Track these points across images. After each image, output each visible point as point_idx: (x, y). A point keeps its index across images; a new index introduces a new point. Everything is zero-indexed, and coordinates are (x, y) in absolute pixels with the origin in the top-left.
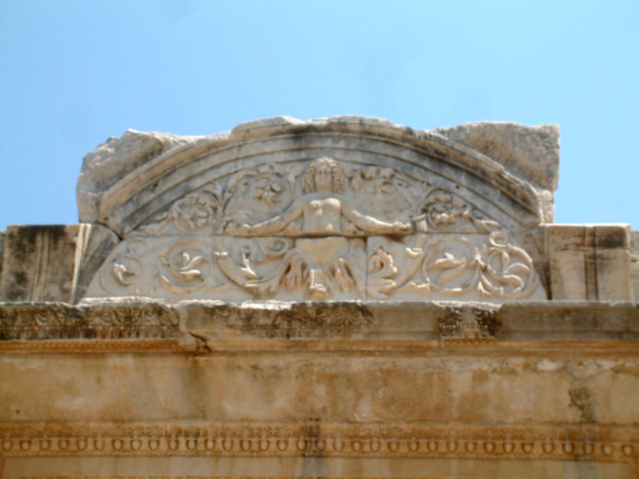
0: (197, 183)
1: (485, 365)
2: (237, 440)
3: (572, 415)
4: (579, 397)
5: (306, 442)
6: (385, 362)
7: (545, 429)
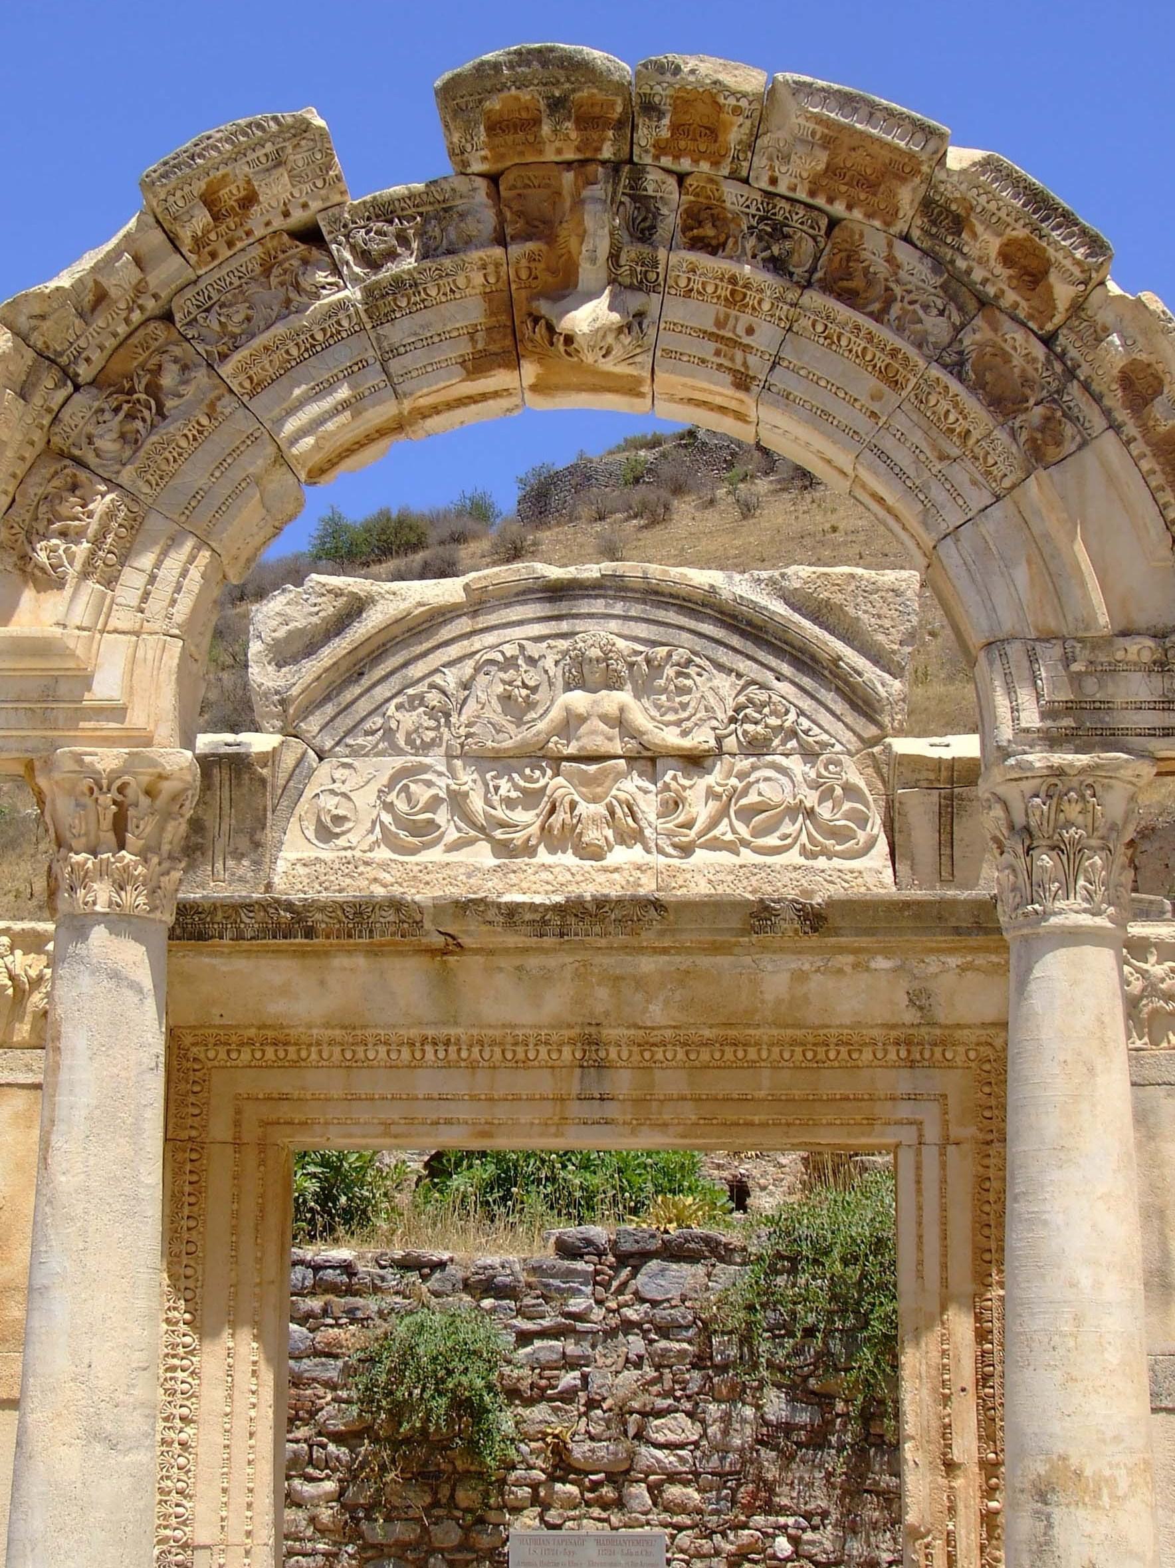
1: (806, 963)
2: (498, 1050)
3: (910, 1016)
4: (917, 999)
5: (585, 1051)
7: (875, 1032)
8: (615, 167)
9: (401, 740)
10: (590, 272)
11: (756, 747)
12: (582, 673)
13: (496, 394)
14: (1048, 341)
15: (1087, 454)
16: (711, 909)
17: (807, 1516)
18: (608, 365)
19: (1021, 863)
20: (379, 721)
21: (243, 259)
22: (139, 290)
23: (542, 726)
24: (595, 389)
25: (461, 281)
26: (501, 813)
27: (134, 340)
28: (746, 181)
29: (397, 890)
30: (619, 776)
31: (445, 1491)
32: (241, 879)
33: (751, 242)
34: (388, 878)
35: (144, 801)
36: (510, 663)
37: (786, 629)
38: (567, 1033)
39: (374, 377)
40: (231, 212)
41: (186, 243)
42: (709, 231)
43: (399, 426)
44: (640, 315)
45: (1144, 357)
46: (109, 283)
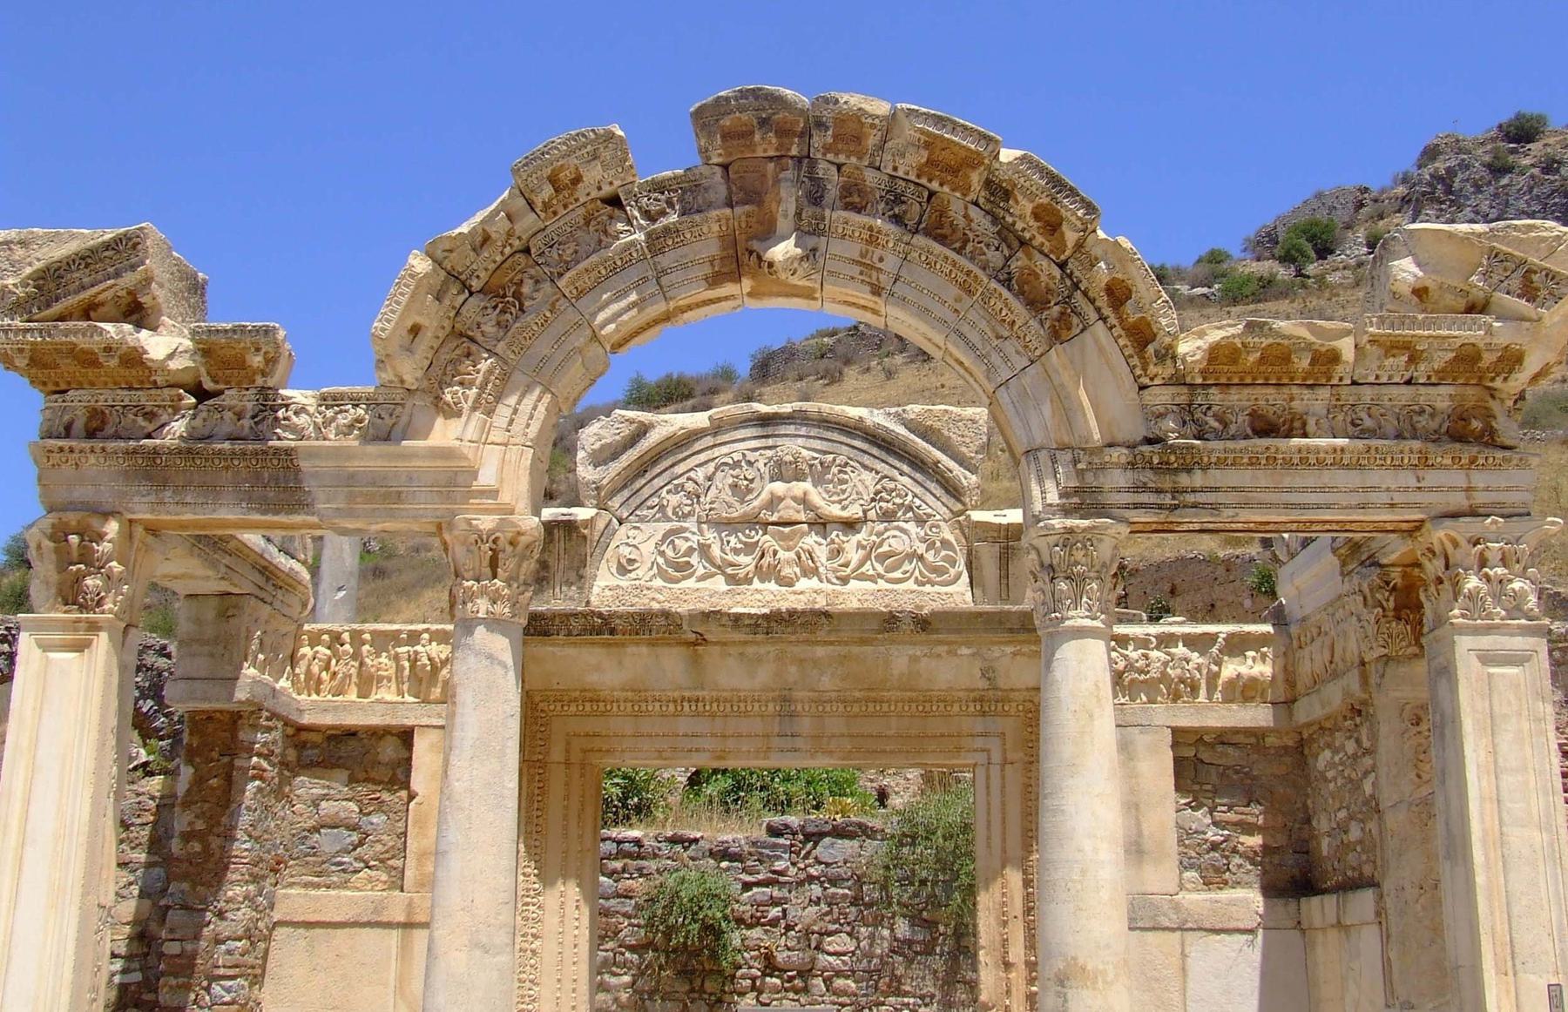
3: (983, 684)
6: (843, 650)
7: (961, 694)
8: (799, 160)
9: (669, 512)
10: (783, 224)
11: (888, 517)
12: (783, 471)
13: (727, 298)
14: (1062, 266)
15: (1086, 334)
16: (860, 617)
17: (922, 997)
18: (795, 280)
19: (1048, 588)
20: (657, 500)
21: (573, 215)
22: (510, 234)
23: (756, 503)
24: (787, 296)
25: (705, 230)
26: (730, 557)
27: (506, 265)
28: (878, 169)
29: (667, 606)
30: (803, 534)
31: (698, 982)
32: (571, 599)
33: (882, 206)
34: (661, 598)
35: (509, 549)
36: (737, 464)
37: (905, 444)
38: (771, 695)
39: (652, 288)
40: (566, 187)
41: (539, 206)
42: (856, 199)
43: (667, 317)
44: (814, 250)
45: (1120, 276)
46: (491, 230)
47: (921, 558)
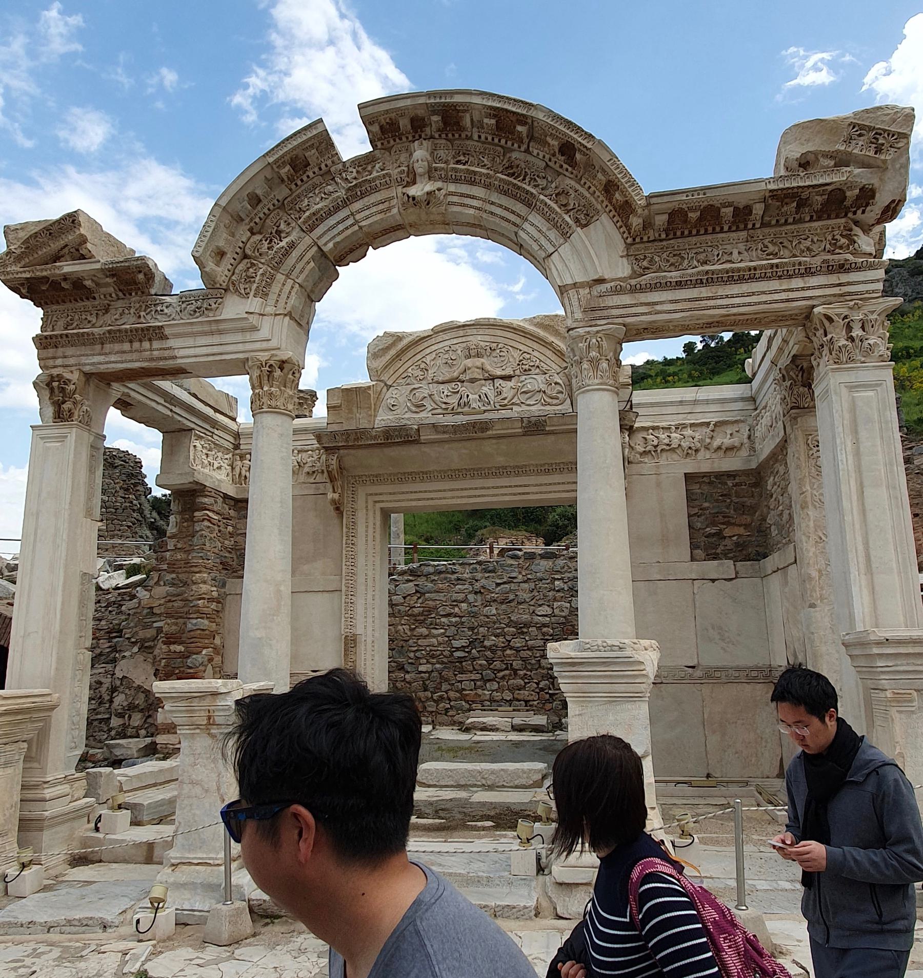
0: (419, 357)
47: (544, 392)
